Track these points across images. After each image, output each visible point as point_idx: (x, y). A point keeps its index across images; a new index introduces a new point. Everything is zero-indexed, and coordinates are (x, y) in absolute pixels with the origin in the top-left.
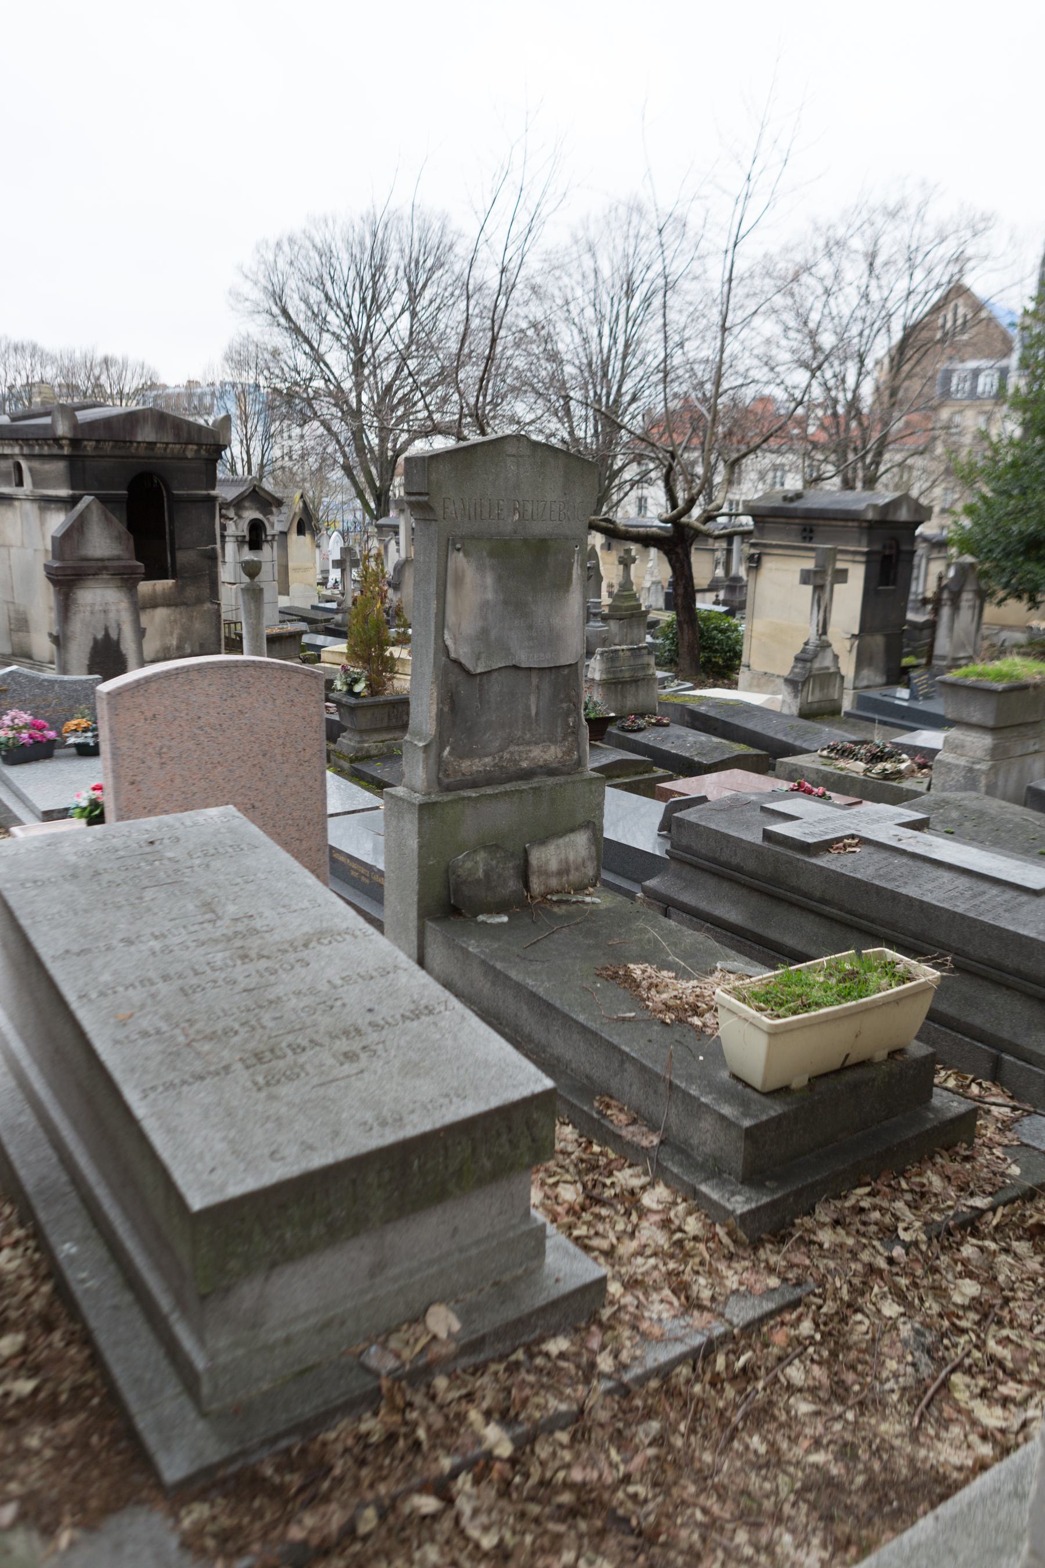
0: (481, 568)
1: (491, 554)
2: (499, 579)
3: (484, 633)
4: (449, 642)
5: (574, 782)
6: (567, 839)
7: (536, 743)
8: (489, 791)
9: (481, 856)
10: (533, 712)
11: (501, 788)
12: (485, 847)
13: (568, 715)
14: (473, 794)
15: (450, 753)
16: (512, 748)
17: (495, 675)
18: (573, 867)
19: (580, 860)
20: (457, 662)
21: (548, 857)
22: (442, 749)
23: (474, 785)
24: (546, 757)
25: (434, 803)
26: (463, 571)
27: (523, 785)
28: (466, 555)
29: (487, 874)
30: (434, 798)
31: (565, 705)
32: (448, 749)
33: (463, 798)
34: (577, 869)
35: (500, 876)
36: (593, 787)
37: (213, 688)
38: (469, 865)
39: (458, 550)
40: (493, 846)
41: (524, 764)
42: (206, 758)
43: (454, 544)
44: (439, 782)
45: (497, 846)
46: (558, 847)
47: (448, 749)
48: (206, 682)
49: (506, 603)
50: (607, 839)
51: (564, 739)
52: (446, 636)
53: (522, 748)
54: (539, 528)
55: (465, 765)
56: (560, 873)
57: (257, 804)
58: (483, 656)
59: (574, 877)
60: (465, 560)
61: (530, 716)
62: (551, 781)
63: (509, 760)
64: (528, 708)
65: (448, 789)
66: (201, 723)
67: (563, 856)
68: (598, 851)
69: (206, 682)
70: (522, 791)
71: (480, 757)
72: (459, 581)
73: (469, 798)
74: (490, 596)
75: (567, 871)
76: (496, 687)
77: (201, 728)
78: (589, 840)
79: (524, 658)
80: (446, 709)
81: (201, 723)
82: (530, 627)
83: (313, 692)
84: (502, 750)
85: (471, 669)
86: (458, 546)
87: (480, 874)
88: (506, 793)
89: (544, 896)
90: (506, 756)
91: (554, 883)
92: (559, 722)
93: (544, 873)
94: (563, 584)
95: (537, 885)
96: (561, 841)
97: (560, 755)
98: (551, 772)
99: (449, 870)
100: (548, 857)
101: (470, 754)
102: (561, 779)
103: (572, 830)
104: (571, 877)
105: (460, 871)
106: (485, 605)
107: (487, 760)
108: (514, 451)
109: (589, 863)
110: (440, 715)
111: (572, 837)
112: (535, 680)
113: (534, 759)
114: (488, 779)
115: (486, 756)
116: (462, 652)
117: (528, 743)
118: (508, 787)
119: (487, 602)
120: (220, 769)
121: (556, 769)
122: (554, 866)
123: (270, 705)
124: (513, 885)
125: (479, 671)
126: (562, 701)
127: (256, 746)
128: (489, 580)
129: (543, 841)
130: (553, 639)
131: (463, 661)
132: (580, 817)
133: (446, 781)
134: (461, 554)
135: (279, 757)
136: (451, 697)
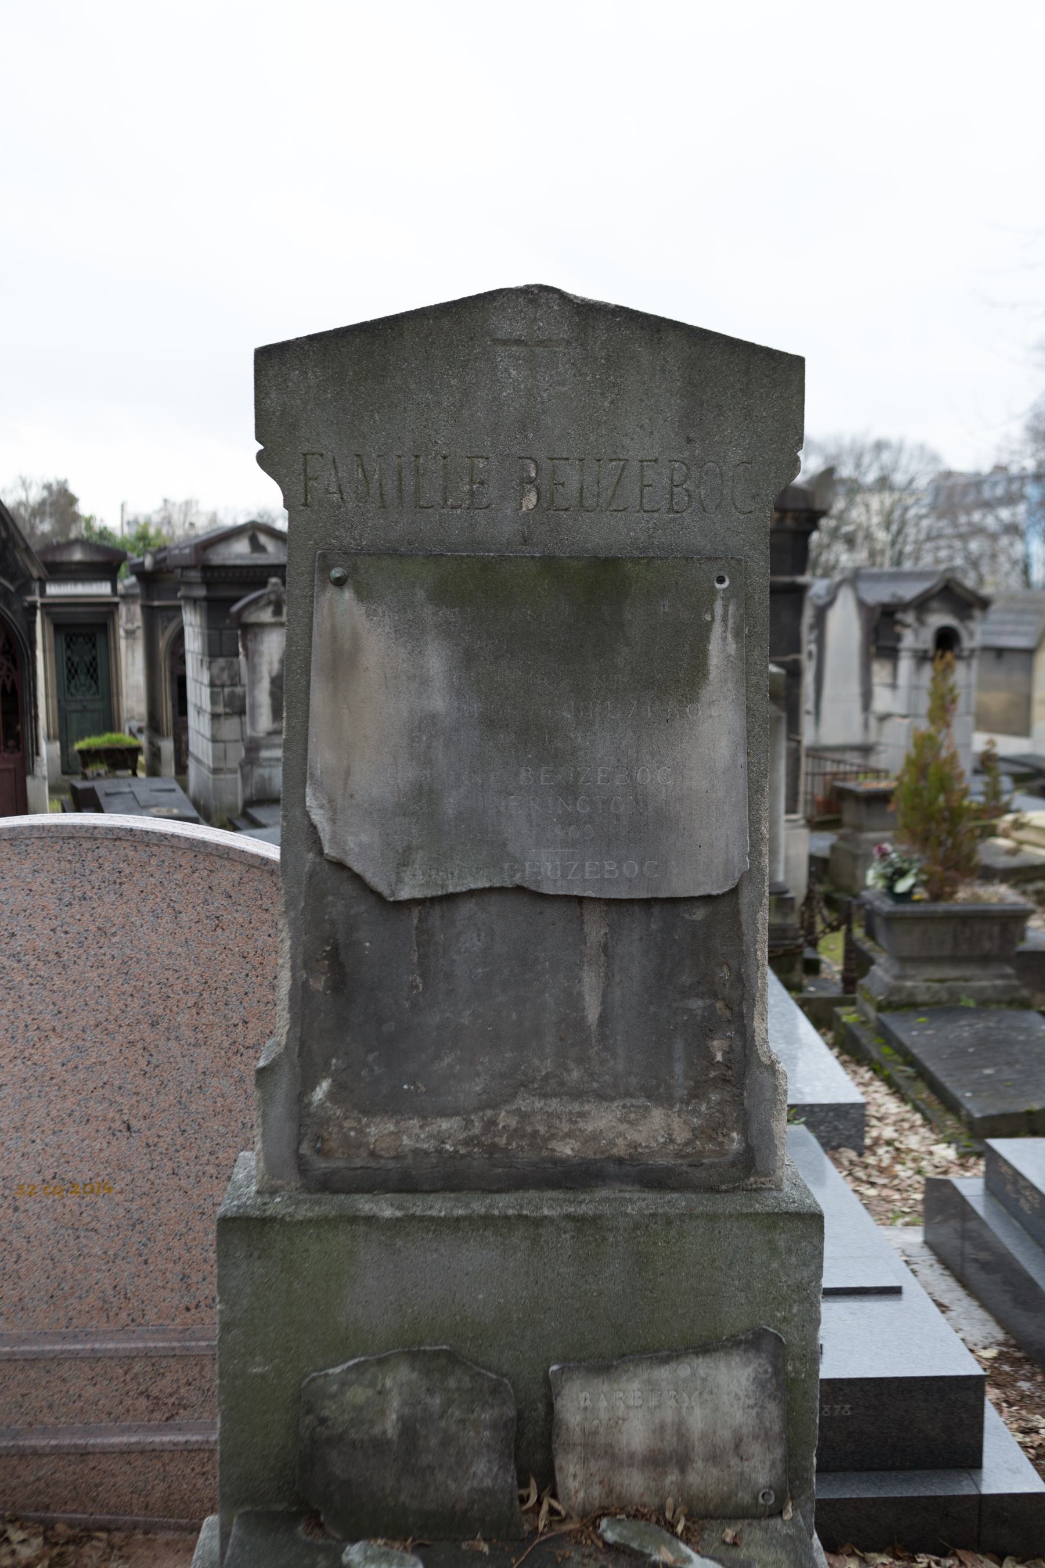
0: (410, 632)
1: (442, 595)
2: (468, 659)
3: (423, 799)
4: (318, 817)
5: (712, 1218)
6: (683, 1370)
7: (602, 1097)
8: (439, 1206)
9: (400, 1377)
10: (592, 1014)
11: (478, 1206)
12: (414, 1356)
13: (707, 1029)
14: (386, 1209)
15: (331, 1095)
16: (522, 1103)
17: (466, 909)
18: (699, 1450)
19: (725, 1434)
20: (340, 866)
21: (619, 1413)
22: (308, 1084)
23: (406, 1184)
24: (633, 1135)
25: (271, 1220)
26: (356, 638)
27: (550, 1205)
28: (363, 594)
29: (408, 1429)
30: (277, 1206)
31: (697, 1004)
32: (325, 1085)
33: (354, 1220)
34: (714, 1457)
35: (446, 1441)
36: (782, 1241)
37: (42, 877)
38: (358, 1394)
39: (339, 583)
40: (439, 1357)
41: (566, 1149)
42: (25, 1017)
43: (326, 569)
44: (302, 1167)
45: (453, 1359)
46: (653, 1387)
47: (325, 1085)
48: (28, 865)
49: (490, 723)
50: (837, 1387)
51: (696, 1093)
52: (309, 801)
53: (554, 1104)
54: (600, 533)
55: (379, 1131)
56: (655, 1461)
57: (135, 1124)
58: (419, 856)
59: (702, 1478)
60: (359, 611)
61: (580, 1024)
62: (642, 1203)
63: (515, 1134)
64: (574, 1001)
65: (326, 1185)
66: (16, 945)
67: (668, 1415)
68: (790, 1419)
69: (28, 865)
70: (539, 1222)
71: (424, 1117)
72: (344, 663)
73: (371, 1220)
74: (439, 703)
75: (682, 1461)
76: (469, 937)
77: (16, 956)
78: (760, 1383)
79: (549, 870)
80: (318, 984)
81: (16, 945)
82: (570, 790)
83: (266, 903)
84: (495, 1106)
85: (383, 888)
86: (336, 573)
87: (390, 1425)
88: (487, 1221)
89: (591, 1518)
90: (505, 1119)
91: (635, 1484)
92: (679, 1047)
93: (604, 1452)
94: (678, 677)
95: (576, 1481)
96: (663, 1373)
97: (681, 1136)
98: (655, 1179)
99: (306, 1402)
101: (394, 1105)
102: (678, 1201)
103: (705, 1348)
104: (693, 1478)
105: (330, 1409)
106: (423, 726)
107: (445, 1124)
108: (519, 330)
109: (755, 1449)
110: (302, 999)
111: (702, 1366)
112: (595, 930)
113: (595, 1136)
114: (450, 1176)
115: (444, 1113)
116: (359, 845)
117: (578, 1094)
118: (504, 1204)
119: (432, 718)
120: (55, 1041)
121: (669, 1171)
122: (636, 1435)
123: (166, 922)
124: (484, 1472)
125: (404, 894)
126: (686, 993)
127: (135, 1004)
128: (436, 662)
129: (604, 1365)
130: (647, 825)
131: (357, 867)
132: (736, 1317)
133: (322, 1165)
134: (347, 594)
135: (187, 1033)
136: (334, 955)
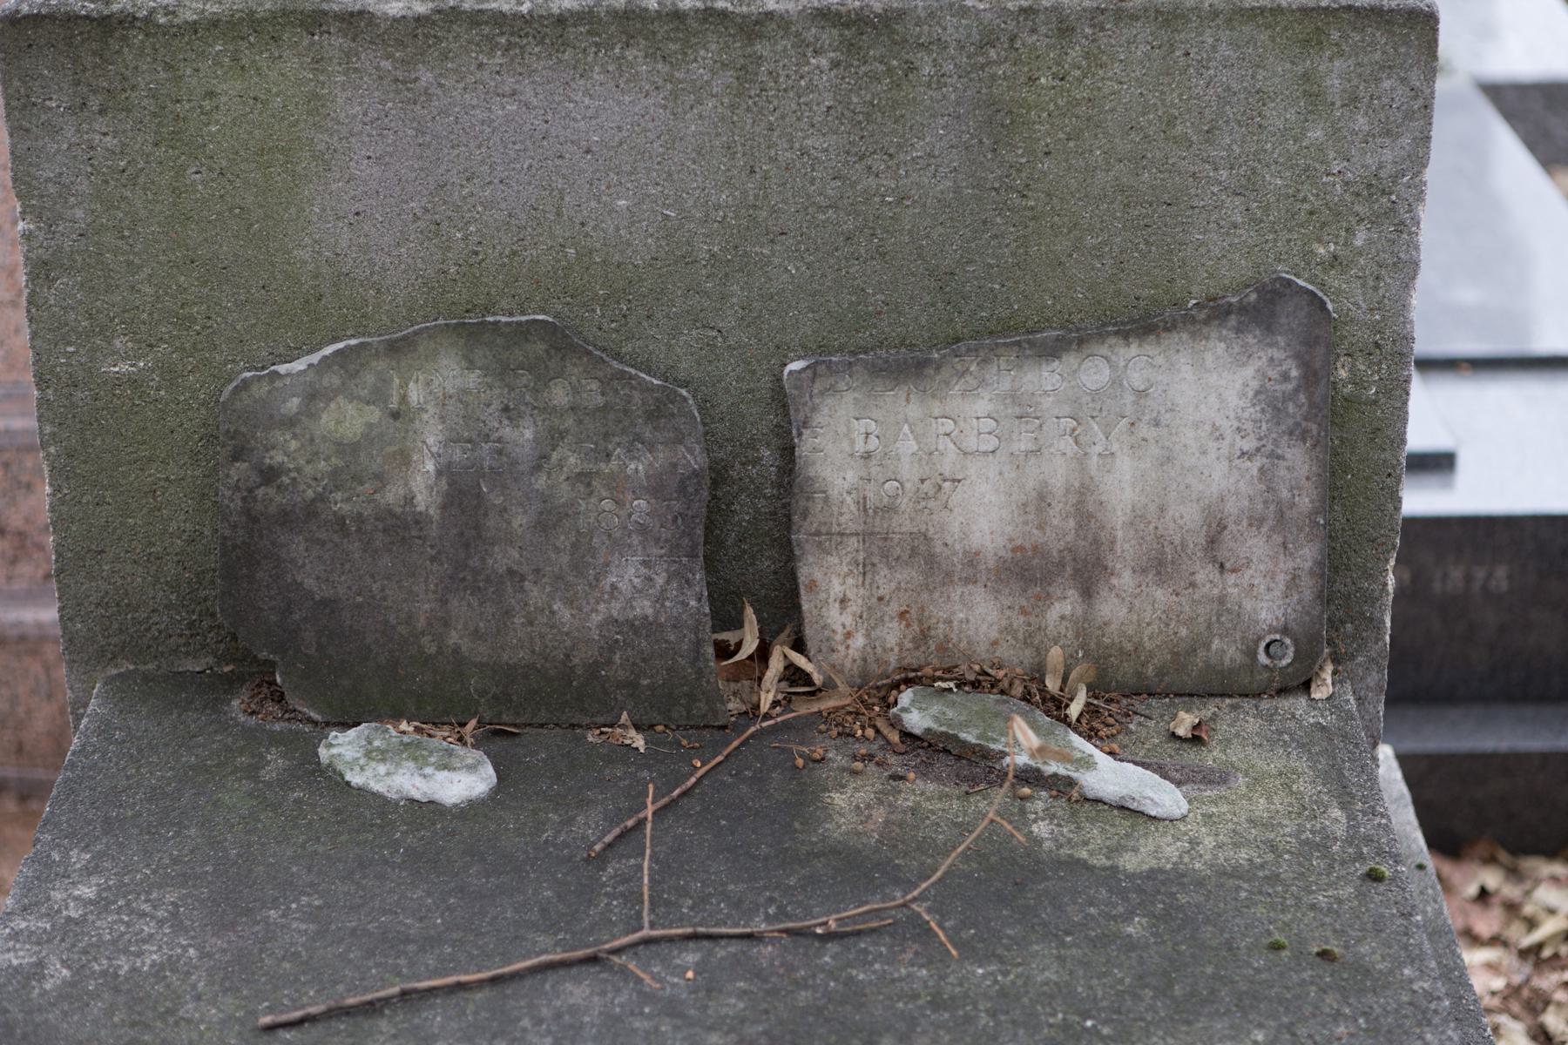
6: (1092, 372)
9: (439, 386)
12: (472, 334)
18: (1126, 547)
19: (1186, 517)
29: (462, 492)
35: (549, 520)
36: (1334, 74)
38: (347, 418)
40: (528, 334)
45: (561, 342)
46: (1024, 410)
56: (1026, 571)
59: (1131, 609)
67: (1057, 472)
75: (1088, 571)
78: (1273, 406)
87: (421, 485)
89: (880, 690)
91: (979, 620)
95: (846, 611)
99: (232, 437)
100: (939, 472)
103: (1145, 324)
104: (1111, 610)
105: (284, 450)
109: (1255, 547)
111: (1137, 363)
122: (983, 516)
124: (636, 586)
132: (1222, 253)
